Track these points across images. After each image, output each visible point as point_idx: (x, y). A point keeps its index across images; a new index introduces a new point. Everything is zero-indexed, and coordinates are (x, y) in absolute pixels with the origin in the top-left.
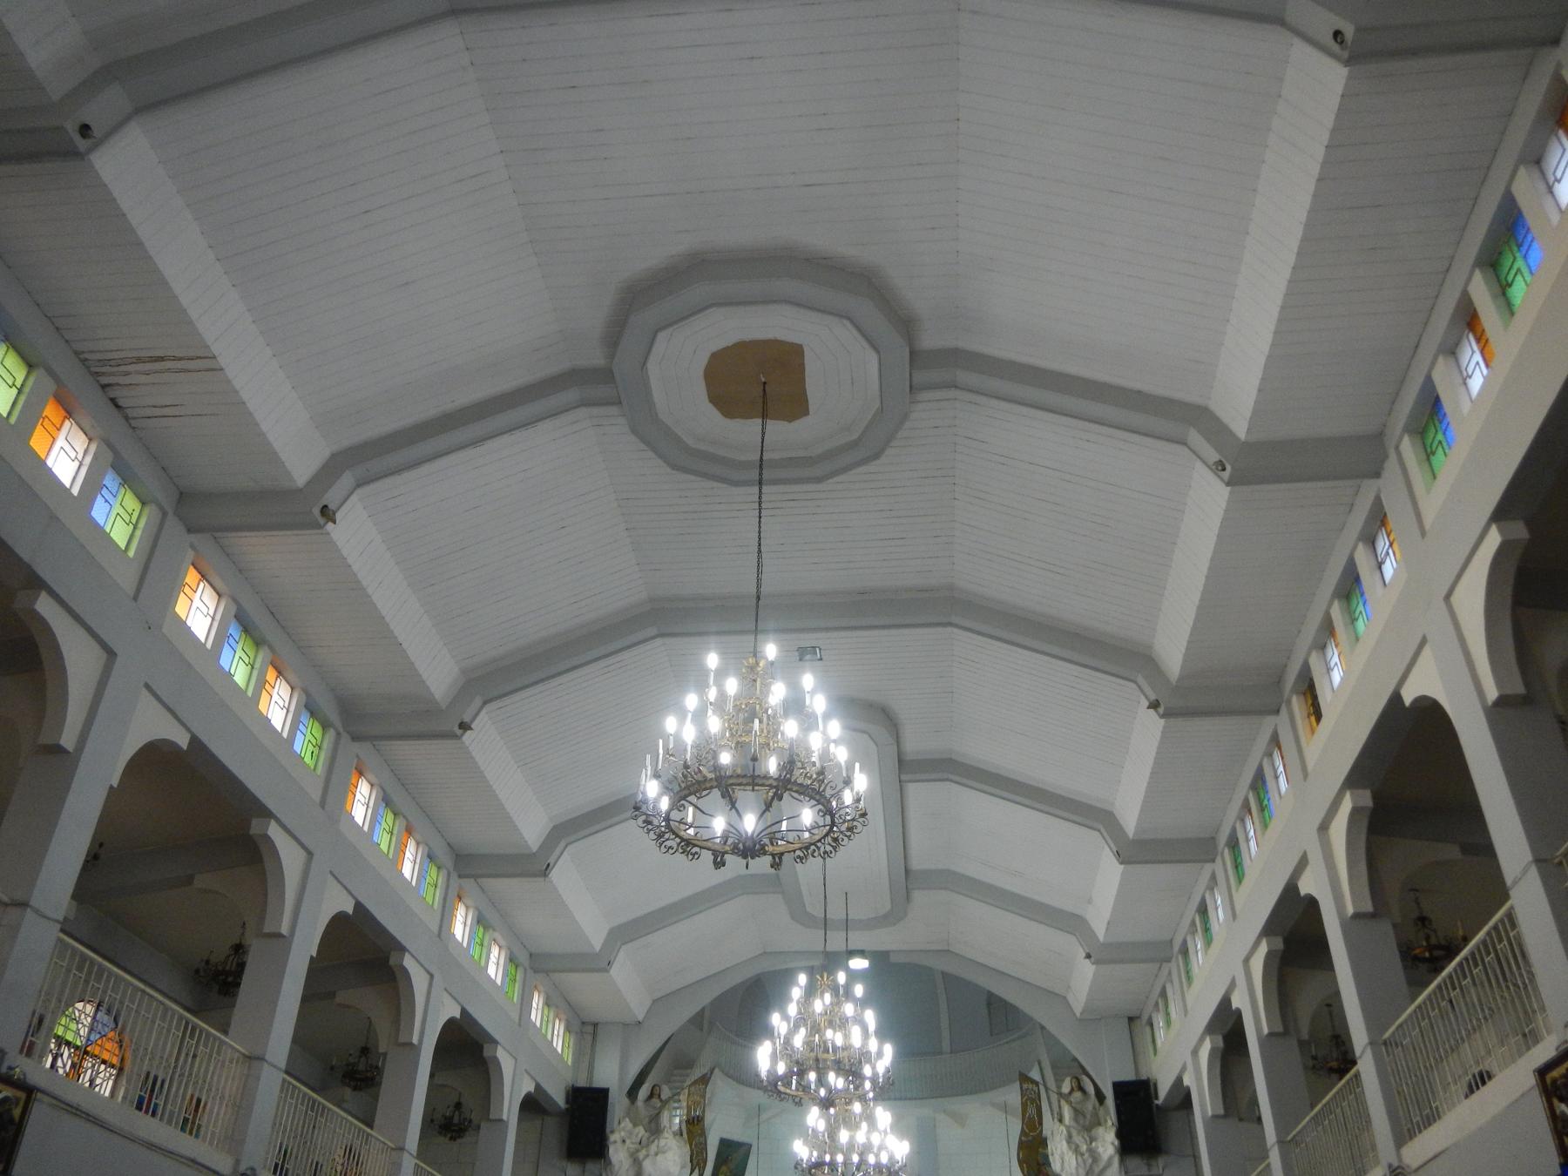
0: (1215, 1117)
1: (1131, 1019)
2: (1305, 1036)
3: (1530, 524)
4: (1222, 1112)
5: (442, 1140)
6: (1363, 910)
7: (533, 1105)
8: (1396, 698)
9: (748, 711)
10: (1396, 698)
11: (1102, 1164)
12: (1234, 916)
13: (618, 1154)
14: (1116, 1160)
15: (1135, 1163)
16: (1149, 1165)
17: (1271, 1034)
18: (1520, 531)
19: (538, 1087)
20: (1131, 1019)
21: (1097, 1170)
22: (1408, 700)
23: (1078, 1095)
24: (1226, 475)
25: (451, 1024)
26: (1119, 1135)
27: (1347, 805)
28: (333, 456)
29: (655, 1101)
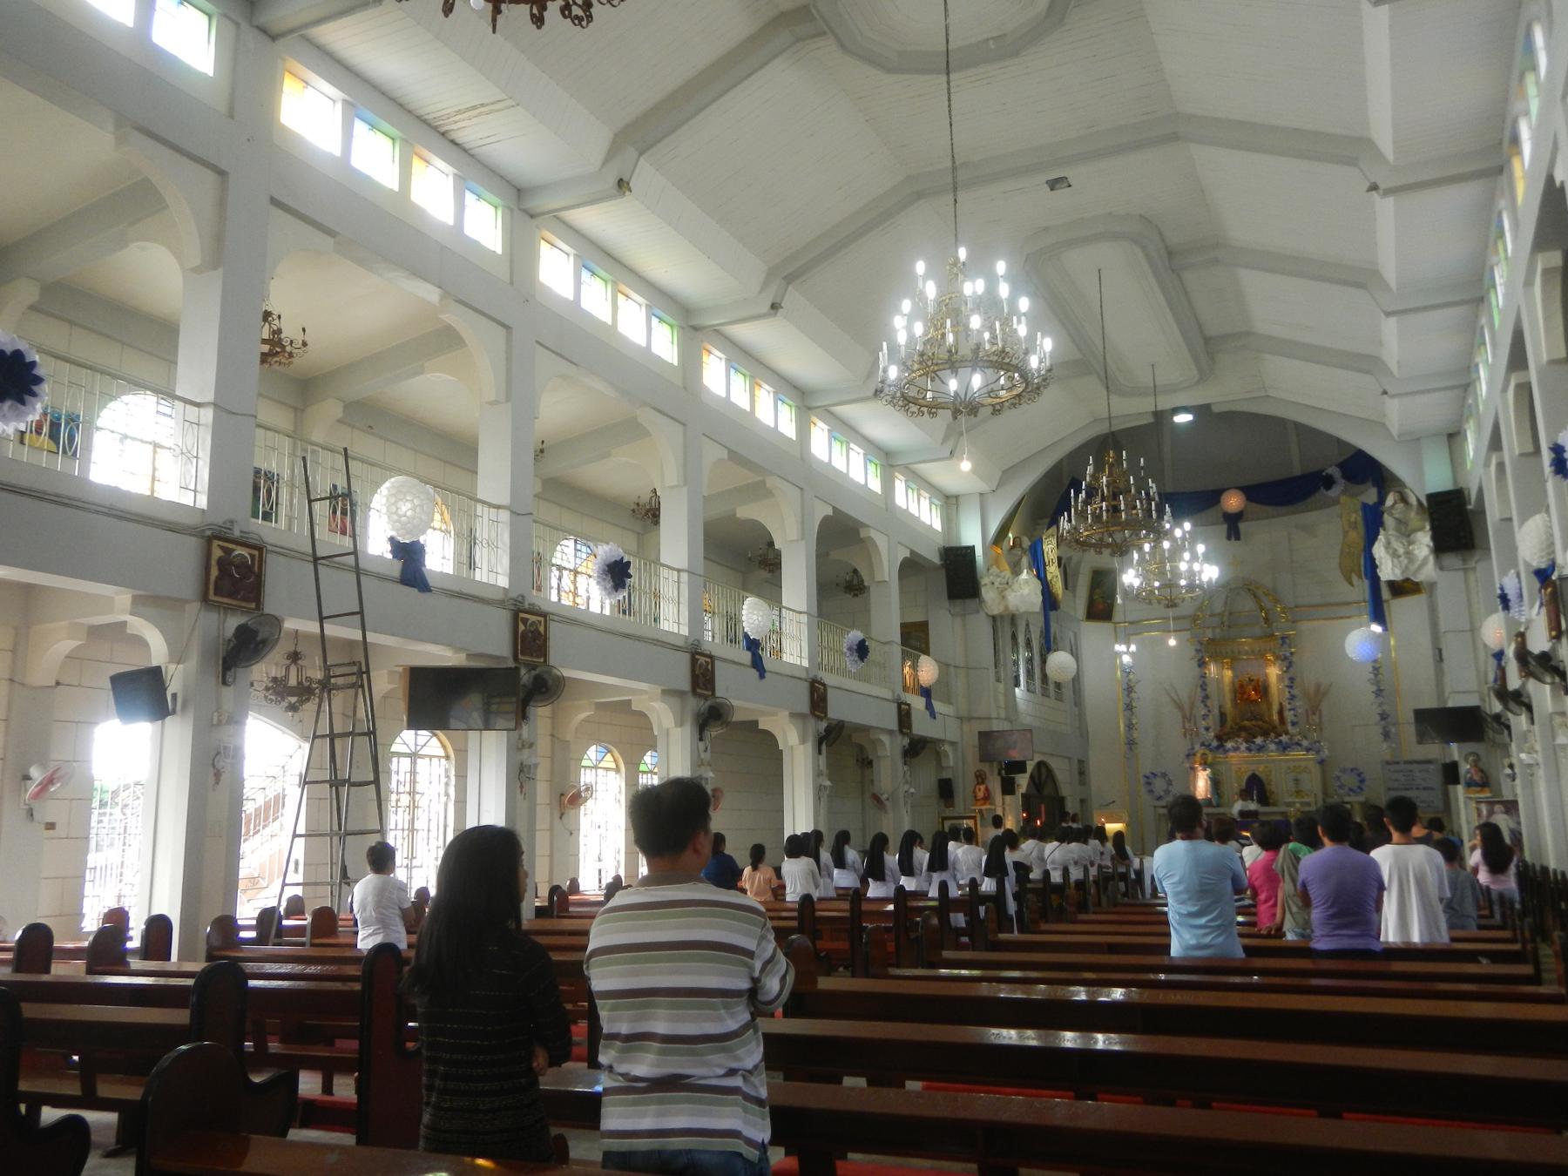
5: (849, 596)
6: (1556, 357)
7: (911, 567)
9: (951, 308)
10: (1550, 179)
13: (988, 594)
14: (1431, 558)
15: (1451, 560)
16: (1464, 561)
17: (1522, 455)
19: (912, 552)
23: (1400, 506)
25: (826, 520)
26: (1434, 538)
28: (616, 135)
29: (1018, 552)
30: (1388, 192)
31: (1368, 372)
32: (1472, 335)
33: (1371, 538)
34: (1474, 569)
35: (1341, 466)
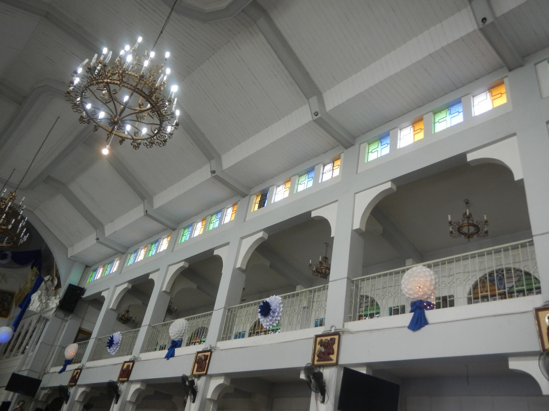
0: (111, 309)
1: (87, 266)
2: (173, 297)
3: (397, 187)
4: (115, 308)
8: (309, 213)
10: (309, 213)
11: (48, 309)
12: (172, 251)
14: (55, 309)
15: (61, 314)
16: (65, 315)
17: (165, 292)
18: (395, 188)
20: (87, 266)
21: (45, 310)
22: (312, 216)
23: (50, 283)
24: (315, 118)
26: (60, 302)
27: (260, 235)
30: (217, 178)
31: (96, 228)
32: (152, 239)
33: (34, 290)
34: (67, 321)
35: (12, 252)
